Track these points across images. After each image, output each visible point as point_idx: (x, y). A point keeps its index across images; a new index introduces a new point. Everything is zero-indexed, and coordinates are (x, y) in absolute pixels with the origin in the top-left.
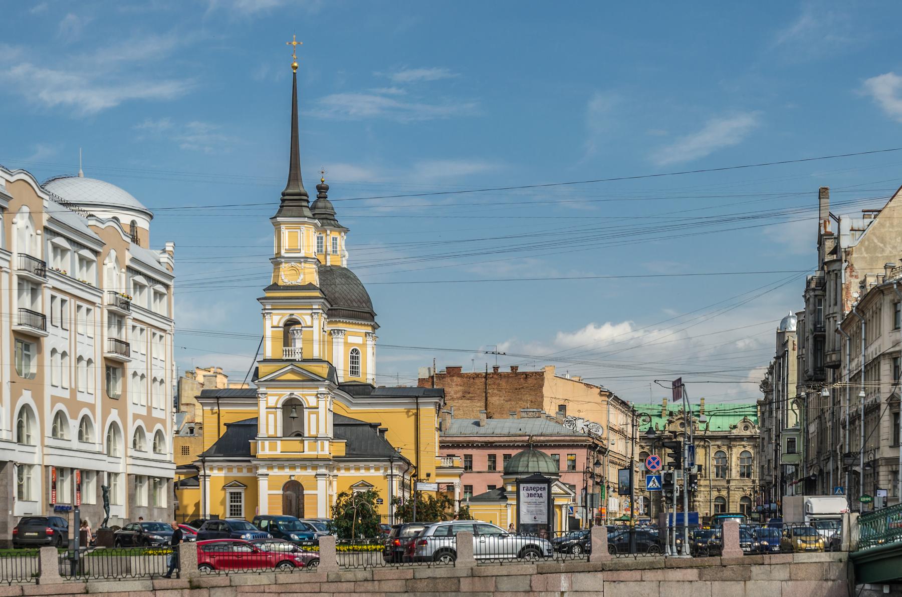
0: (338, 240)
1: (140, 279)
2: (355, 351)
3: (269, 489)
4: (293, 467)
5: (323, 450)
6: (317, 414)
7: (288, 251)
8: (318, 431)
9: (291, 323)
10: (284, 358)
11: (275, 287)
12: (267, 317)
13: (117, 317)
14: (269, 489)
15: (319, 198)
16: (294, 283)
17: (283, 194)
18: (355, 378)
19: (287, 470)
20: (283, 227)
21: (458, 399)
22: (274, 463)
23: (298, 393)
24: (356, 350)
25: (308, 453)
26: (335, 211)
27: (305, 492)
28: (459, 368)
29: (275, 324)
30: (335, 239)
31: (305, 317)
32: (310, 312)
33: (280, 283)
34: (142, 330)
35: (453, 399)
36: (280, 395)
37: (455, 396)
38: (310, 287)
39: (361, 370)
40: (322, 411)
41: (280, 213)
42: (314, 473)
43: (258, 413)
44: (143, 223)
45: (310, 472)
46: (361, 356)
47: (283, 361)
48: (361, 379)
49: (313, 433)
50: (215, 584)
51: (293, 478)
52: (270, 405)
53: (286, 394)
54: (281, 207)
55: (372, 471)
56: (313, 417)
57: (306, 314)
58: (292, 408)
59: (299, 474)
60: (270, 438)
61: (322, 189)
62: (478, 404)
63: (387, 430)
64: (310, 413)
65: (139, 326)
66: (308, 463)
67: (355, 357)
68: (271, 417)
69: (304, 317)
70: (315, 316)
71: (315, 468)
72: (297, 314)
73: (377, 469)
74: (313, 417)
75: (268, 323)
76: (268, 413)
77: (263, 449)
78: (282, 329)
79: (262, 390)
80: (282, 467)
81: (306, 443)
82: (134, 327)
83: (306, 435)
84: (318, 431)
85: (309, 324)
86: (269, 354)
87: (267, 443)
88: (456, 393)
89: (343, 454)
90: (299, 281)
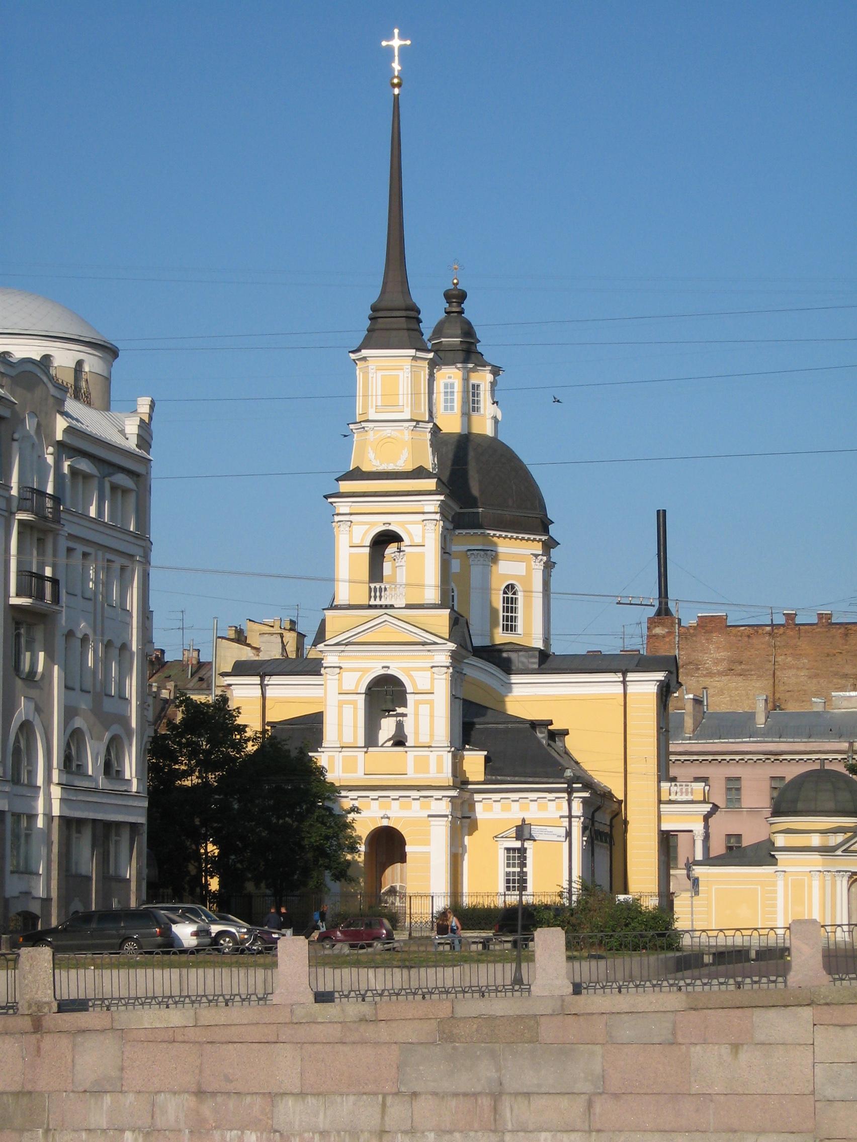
0: (482, 388)
1: (84, 465)
6: (431, 703)
8: (432, 735)
9: (385, 540)
10: (372, 602)
11: (357, 474)
12: (344, 527)
13: (37, 533)
17: (374, 309)
21: (720, 673)
25: (413, 776)
27: (408, 849)
28: (722, 620)
29: (356, 541)
33: (365, 469)
34: (85, 555)
35: (710, 674)
36: (365, 671)
37: (714, 669)
39: (520, 624)
41: (367, 343)
42: (425, 813)
43: (322, 701)
44: (93, 363)
46: (520, 596)
47: (370, 607)
49: (424, 739)
50: (91, 1027)
51: (385, 823)
52: (346, 687)
54: (370, 330)
56: (424, 709)
61: (456, 297)
62: (758, 684)
63: (565, 733)
64: (417, 703)
65: (80, 548)
66: (415, 794)
68: (348, 710)
76: (341, 705)
78: (367, 550)
79: (330, 659)
82: (70, 550)
84: (432, 735)
85: (418, 541)
86: (343, 595)
88: (717, 662)
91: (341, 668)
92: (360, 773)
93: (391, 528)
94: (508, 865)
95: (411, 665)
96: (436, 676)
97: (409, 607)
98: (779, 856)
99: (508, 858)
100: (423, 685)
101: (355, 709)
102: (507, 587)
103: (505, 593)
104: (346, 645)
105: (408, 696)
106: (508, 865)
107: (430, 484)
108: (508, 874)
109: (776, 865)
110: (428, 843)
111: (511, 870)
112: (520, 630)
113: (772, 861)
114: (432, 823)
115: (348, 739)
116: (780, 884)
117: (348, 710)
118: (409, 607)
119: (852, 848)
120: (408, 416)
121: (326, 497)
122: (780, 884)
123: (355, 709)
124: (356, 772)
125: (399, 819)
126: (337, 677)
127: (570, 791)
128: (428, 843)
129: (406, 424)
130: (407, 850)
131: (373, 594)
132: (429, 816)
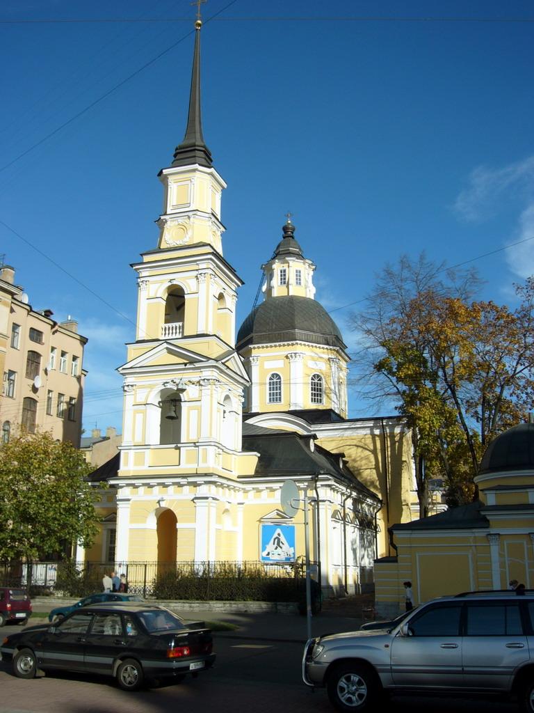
2: (316, 376)
3: (132, 521)
5: (205, 461)
6: (199, 409)
7: (175, 207)
14: (132, 521)
15: (284, 238)
20: (171, 179)
25: (187, 467)
27: (179, 525)
29: (152, 295)
30: (298, 273)
32: (195, 273)
45: (188, 492)
49: (193, 438)
56: (194, 414)
57: (190, 278)
58: (171, 403)
59: (173, 498)
69: (187, 282)
72: (179, 280)
75: (144, 294)
76: (136, 412)
77: (126, 464)
87: (132, 452)
90: (185, 240)
93: (174, 282)
98: (491, 516)
102: (314, 376)
103: (312, 379)
105: (182, 404)
109: (487, 527)
113: (484, 523)
116: (495, 549)
121: (132, 265)
122: (495, 549)
125: (173, 501)
127: (315, 480)
130: (177, 527)
131: (164, 332)
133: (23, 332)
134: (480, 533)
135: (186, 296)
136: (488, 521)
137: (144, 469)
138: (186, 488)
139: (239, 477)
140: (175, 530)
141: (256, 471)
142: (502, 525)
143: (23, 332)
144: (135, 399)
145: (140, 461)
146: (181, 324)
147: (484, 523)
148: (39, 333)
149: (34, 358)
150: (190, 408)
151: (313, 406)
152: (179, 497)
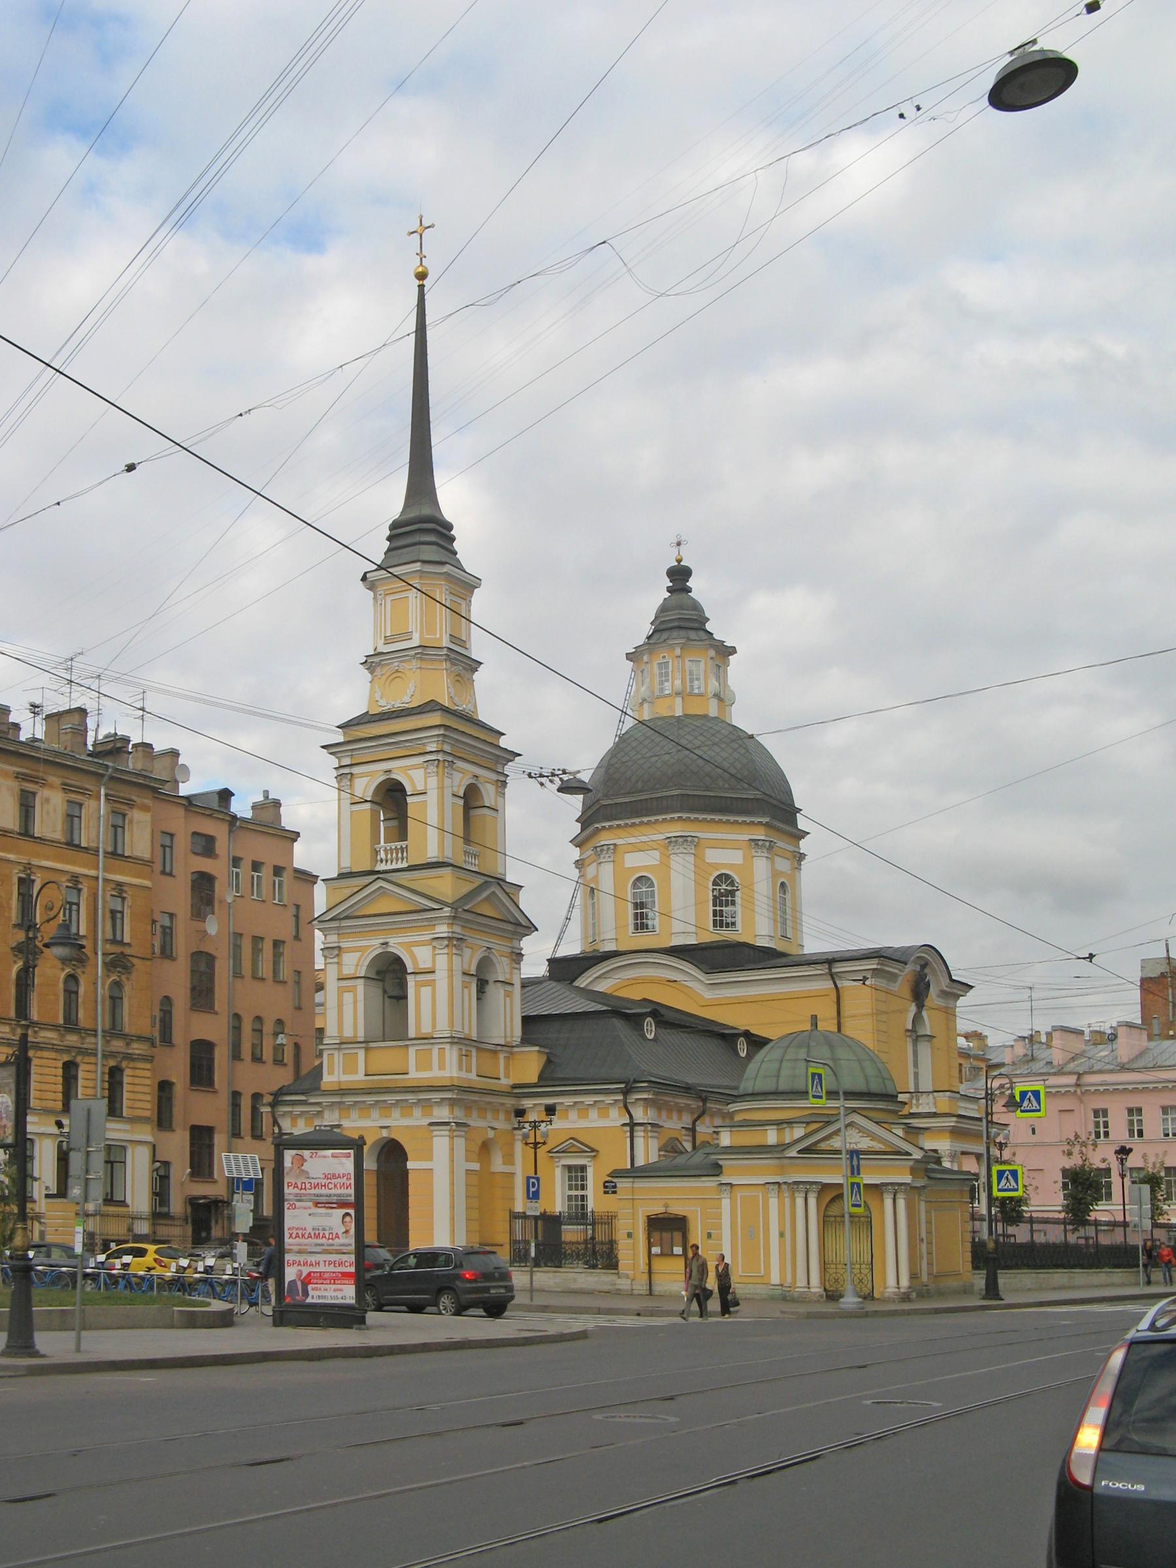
4: (385, 1107)
5: (442, 1067)
6: (431, 983)
8: (434, 1026)
16: (398, 705)
18: (726, 935)
19: (375, 1113)
22: (349, 1099)
23: (397, 945)
24: (727, 876)
25: (416, 1075)
26: (707, 615)
31: (412, 773)
38: (431, 706)
40: (441, 977)
45: (418, 1119)
48: (740, 934)
49: (426, 1029)
51: (385, 1133)
52: (348, 971)
53: (372, 946)
55: (593, 1114)
58: (390, 975)
59: (401, 1124)
60: (343, 1043)
64: (419, 985)
67: (725, 891)
69: (415, 776)
70: (432, 769)
71: (427, 1105)
73: (603, 1111)
74: (426, 992)
76: (341, 991)
77: (331, 1072)
80: (364, 1109)
81: (412, 1051)
83: (412, 1033)
84: (434, 1026)
85: (420, 787)
87: (338, 1057)
89: (535, 1079)
91: (339, 948)
92: (360, 1076)
93: (394, 776)
94: (570, 1188)
95: (407, 940)
96: (438, 951)
97: (411, 868)
99: (570, 1179)
100: (425, 964)
101: (355, 997)
103: (715, 883)
104: (347, 918)
105: (409, 978)
106: (570, 1188)
107: (435, 719)
108: (570, 1198)
110: (430, 1158)
111: (574, 1193)
112: (739, 926)
113: (716, 1169)
114: (435, 1133)
115: (348, 1033)
117: (348, 997)
118: (411, 868)
119: (823, 1146)
120: (415, 642)
122: (726, 1203)
123: (355, 997)
124: (356, 1073)
126: (335, 960)
128: (430, 1158)
129: (412, 653)
132: (431, 1124)
133: (182, 843)
134: (709, 1183)
135: (409, 800)
136: (721, 1167)
137: (358, 1077)
138: (417, 1112)
139: (515, 1086)
140: (405, 1173)
141: (541, 1077)
142: (736, 1173)
143: (182, 843)
144: (340, 971)
145: (350, 1068)
146: (404, 844)
147: (716, 1169)
148: (210, 840)
149: (203, 884)
150: (419, 985)
151: (711, 935)
152: (406, 1122)
